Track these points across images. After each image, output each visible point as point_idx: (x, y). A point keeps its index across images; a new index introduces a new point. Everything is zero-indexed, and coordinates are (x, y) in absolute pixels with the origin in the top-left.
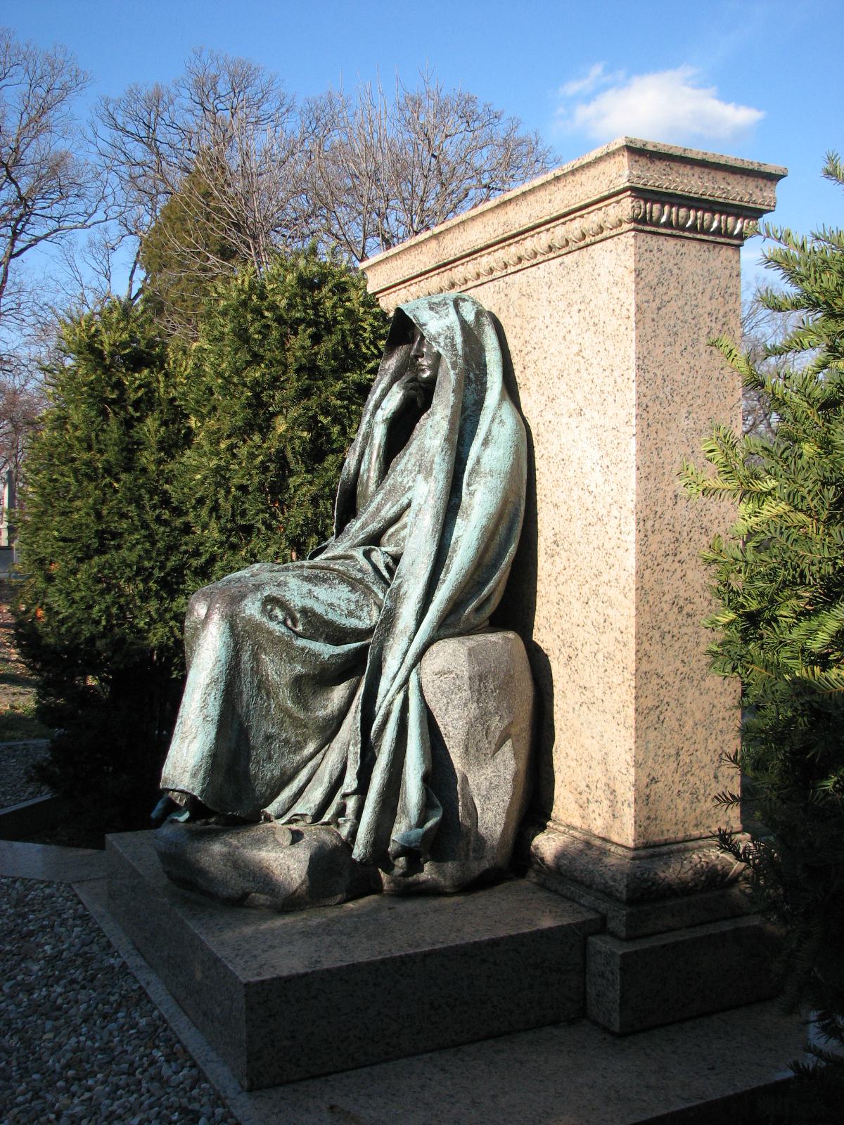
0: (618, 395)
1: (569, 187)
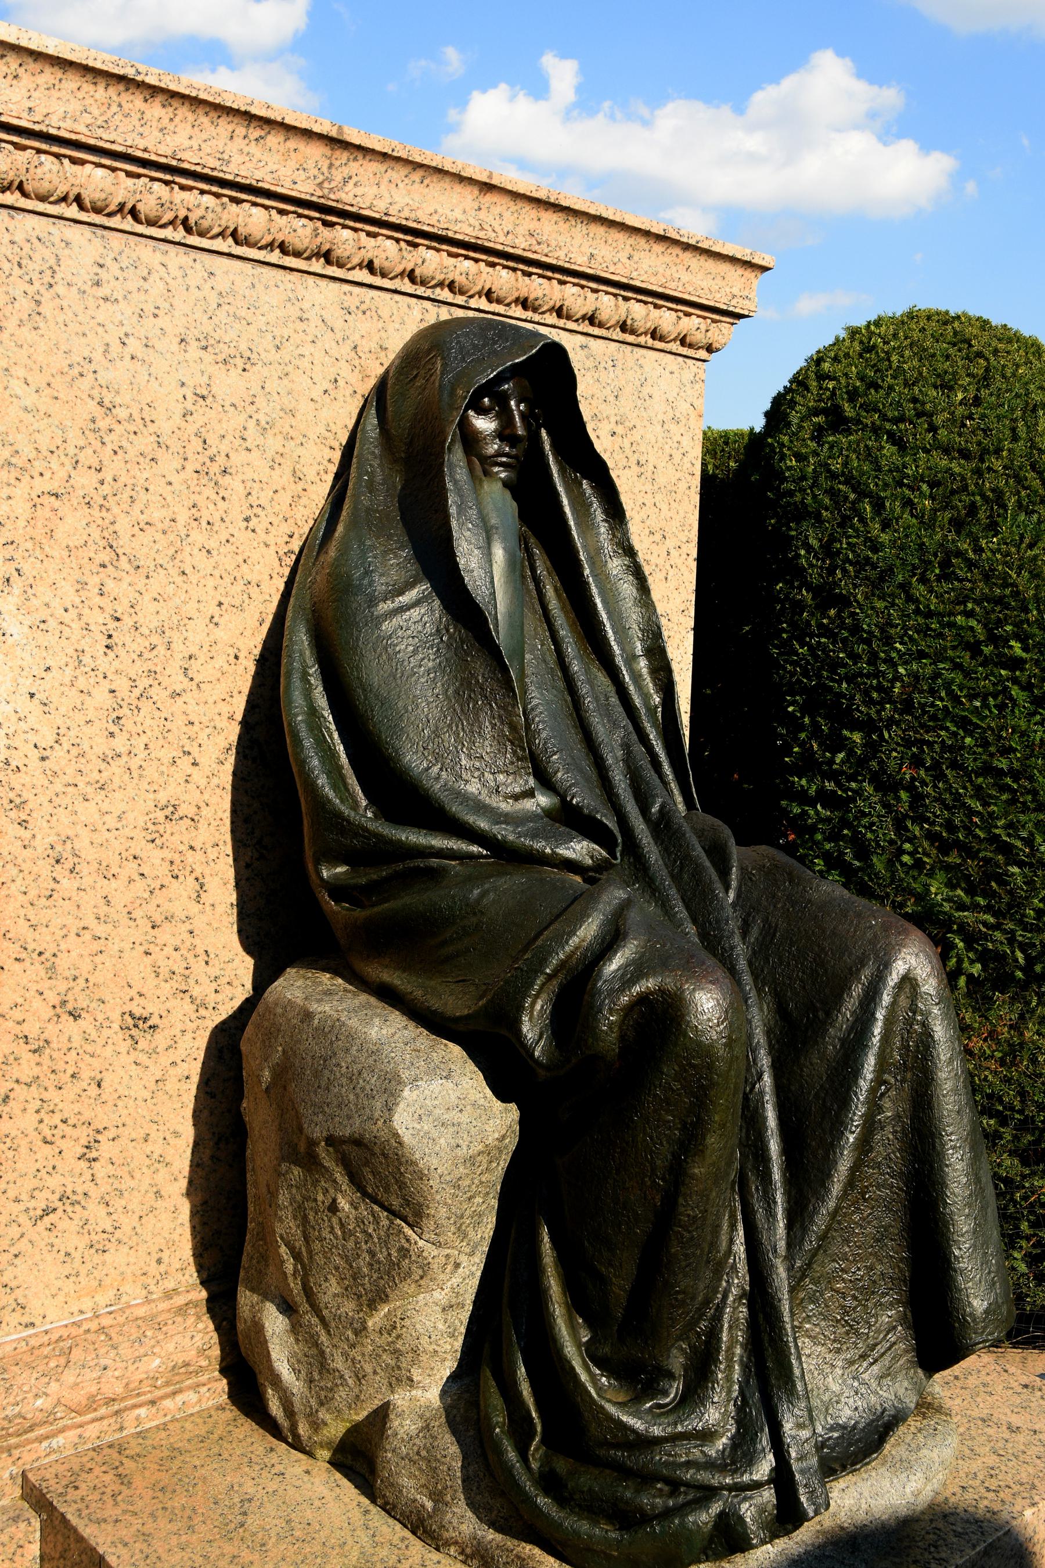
0: (671, 572)
1: (667, 259)
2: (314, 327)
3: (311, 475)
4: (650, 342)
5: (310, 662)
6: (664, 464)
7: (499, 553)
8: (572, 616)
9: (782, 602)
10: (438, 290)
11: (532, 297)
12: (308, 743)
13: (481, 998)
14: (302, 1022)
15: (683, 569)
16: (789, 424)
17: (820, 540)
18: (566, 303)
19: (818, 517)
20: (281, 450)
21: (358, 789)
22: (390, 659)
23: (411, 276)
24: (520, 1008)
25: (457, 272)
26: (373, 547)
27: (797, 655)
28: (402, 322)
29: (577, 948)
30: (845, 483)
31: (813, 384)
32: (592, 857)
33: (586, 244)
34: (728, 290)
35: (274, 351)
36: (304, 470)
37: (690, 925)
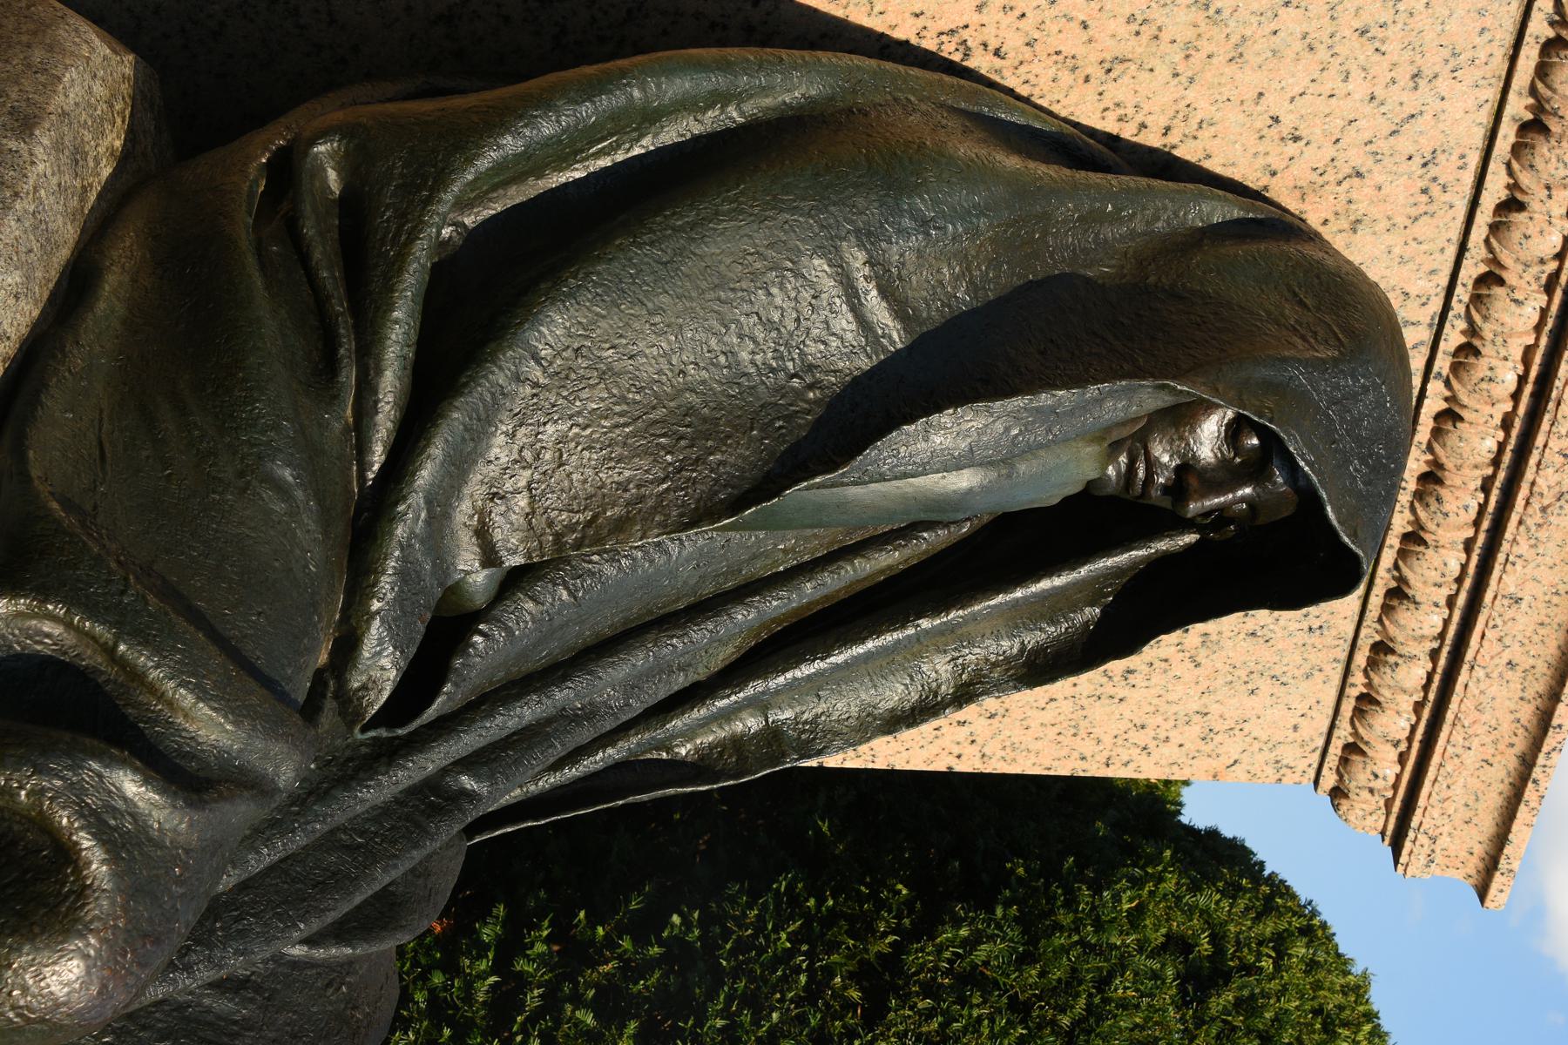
1: (1506, 727)
2: (1402, 98)
3: (1115, 92)
4: (1353, 692)
5: (750, 107)
6: (1127, 714)
7: (964, 480)
8: (842, 596)
9: (874, 895)
10: (1462, 325)
11: (1443, 492)
12: (587, 111)
13: (67, 504)
14: (13, 112)
15: (934, 749)
16: (1195, 888)
17: (986, 963)
18: (1430, 552)
19: (1025, 960)
20: (1165, 37)
21: (497, 208)
22: (754, 276)
23: (1491, 278)
24: (43, 593)
25: (1494, 362)
26: (974, 233)
27: (776, 930)
28: (1400, 254)
29: (170, 704)
30: (1089, 1007)
31: (1268, 927)
32: (364, 687)
33: (1539, 590)
34: (1445, 830)
35: (1357, 24)
36: (1126, 79)
37: (233, 881)
